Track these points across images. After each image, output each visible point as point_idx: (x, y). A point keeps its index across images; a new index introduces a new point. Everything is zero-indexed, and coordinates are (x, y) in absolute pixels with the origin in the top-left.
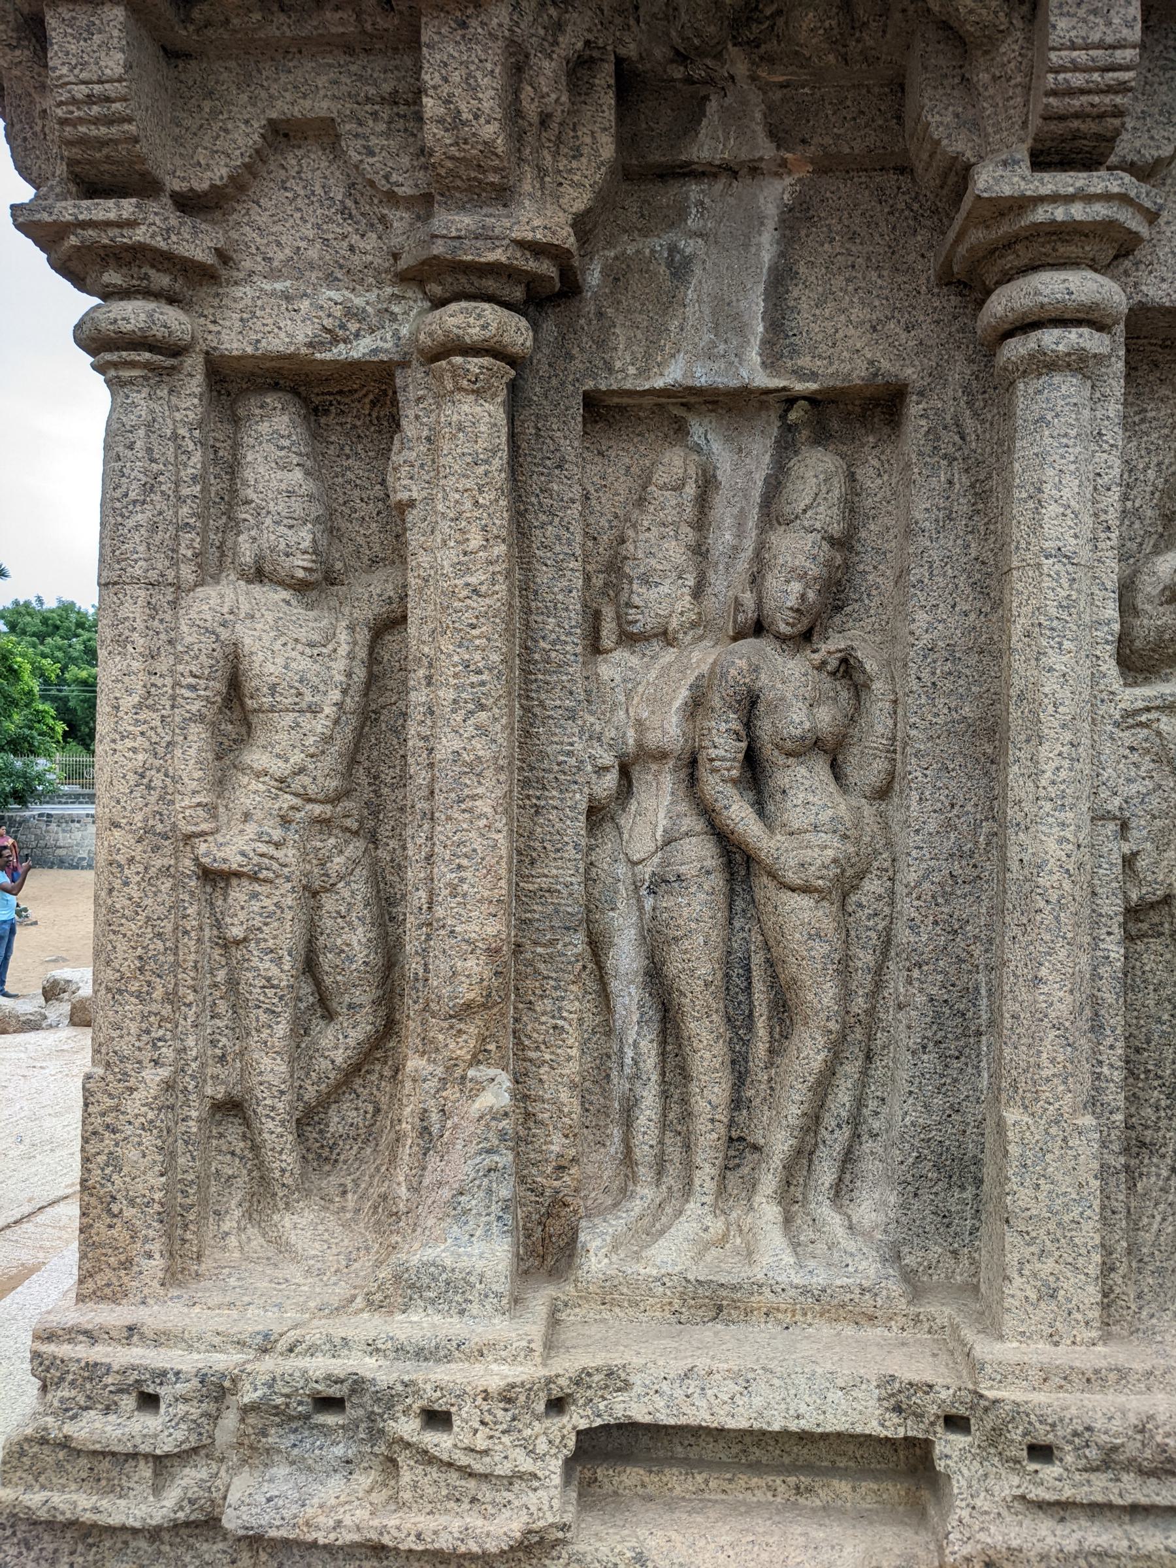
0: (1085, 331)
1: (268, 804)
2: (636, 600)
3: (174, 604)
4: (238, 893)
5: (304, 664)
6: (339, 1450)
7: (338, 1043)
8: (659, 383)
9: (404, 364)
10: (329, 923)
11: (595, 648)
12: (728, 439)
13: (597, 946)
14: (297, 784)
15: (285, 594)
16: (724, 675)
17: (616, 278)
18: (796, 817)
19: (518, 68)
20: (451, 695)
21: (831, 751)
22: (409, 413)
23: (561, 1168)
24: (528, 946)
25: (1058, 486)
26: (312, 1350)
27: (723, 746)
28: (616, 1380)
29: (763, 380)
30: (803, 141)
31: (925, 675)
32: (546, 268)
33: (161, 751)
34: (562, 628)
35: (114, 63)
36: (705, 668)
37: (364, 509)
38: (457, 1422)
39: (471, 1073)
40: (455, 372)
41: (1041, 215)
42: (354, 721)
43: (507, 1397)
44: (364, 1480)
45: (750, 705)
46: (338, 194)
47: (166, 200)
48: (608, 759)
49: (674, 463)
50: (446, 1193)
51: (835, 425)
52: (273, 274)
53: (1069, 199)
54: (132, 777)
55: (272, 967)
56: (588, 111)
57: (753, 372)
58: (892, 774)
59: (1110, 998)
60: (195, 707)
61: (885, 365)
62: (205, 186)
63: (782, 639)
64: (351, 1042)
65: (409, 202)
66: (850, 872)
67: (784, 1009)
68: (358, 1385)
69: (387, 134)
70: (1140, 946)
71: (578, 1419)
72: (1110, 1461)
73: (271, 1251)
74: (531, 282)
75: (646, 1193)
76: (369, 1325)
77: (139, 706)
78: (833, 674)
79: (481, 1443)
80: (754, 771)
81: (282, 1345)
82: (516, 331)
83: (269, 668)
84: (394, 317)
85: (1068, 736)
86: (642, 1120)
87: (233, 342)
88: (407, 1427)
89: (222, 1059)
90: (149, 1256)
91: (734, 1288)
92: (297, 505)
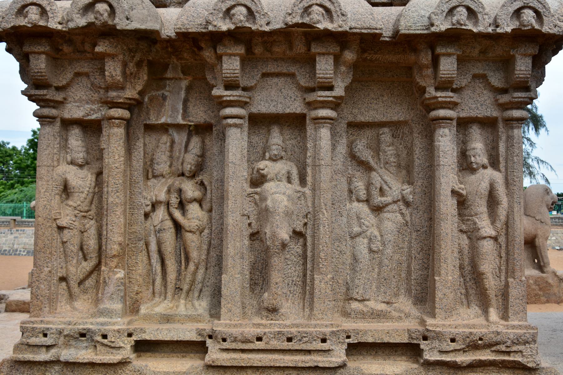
0: (236, 119)
1: (72, 213)
2: (156, 168)
3: (53, 170)
4: (66, 231)
5: (81, 182)
6: (85, 345)
7: (87, 266)
8: (160, 122)
9: (103, 120)
10: (86, 239)
11: (148, 179)
12: (177, 133)
13: (147, 245)
14: (78, 208)
15: (77, 167)
16: (173, 185)
17: (151, 100)
18: (189, 216)
19: (125, 65)
20: (111, 189)
21: (200, 202)
22: (104, 130)
23: (137, 293)
24: (130, 245)
25: (232, 149)
26: (80, 324)
27: (174, 201)
28: (143, 331)
29: (182, 122)
30: (189, 74)
31: (216, 185)
32: (132, 102)
33: (49, 201)
34: (138, 175)
35: (43, 66)
36: (171, 183)
37: (95, 148)
38: (108, 336)
39: (115, 270)
40: (113, 123)
41: (225, 99)
42: (92, 195)
43: (118, 331)
44: (89, 351)
45: (180, 191)
46: (89, 86)
47: (53, 88)
48: (149, 203)
49: (165, 138)
50: (109, 295)
51: (200, 130)
52: (75, 102)
53: (230, 96)
54: (43, 207)
55: (73, 247)
56: (141, 70)
57: (180, 120)
58: (212, 207)
59: (245, 252)
60: (57, 192)
61: (208, 120)
62: (61, 85)
63: (188, 177)
64: (91, 265)
65: (104, 89)
66: (201, 228)
67: (188, 259)
68: (89, 330)
69: (99, 75)
70: (255, 242)
71: (134, 338)
72: (235, 340)
73: (72, 309)
74: (129, 104)
75: (157, 299)
76: (91, 320)
77: (45, 192)
78: (200, 184)
79: (113, 340)
80: (182, 206)
81: (73, 323)
82: (126, 114)
83: (73, 183)
84: (101, 110)
85: (234, 199)
86: (156, 283)
87: (67, 116)
88: (99, 338)
89: (62, 268)
90: (45, 307)
91: (171, 316)
92: (80, 149)
